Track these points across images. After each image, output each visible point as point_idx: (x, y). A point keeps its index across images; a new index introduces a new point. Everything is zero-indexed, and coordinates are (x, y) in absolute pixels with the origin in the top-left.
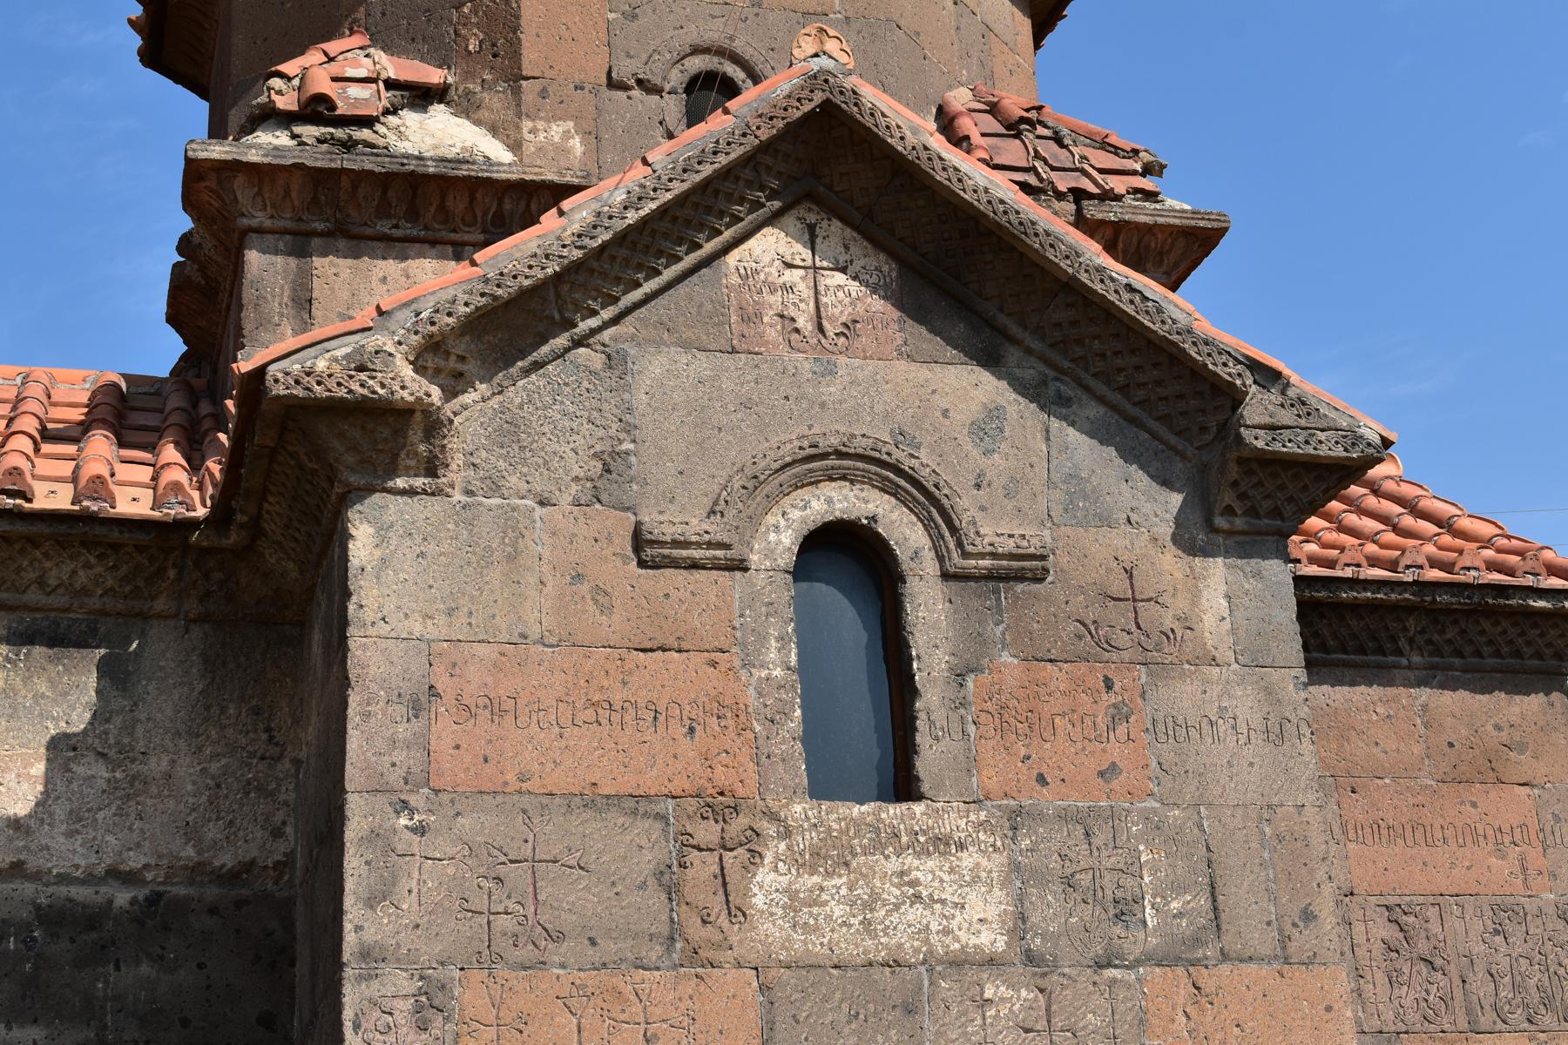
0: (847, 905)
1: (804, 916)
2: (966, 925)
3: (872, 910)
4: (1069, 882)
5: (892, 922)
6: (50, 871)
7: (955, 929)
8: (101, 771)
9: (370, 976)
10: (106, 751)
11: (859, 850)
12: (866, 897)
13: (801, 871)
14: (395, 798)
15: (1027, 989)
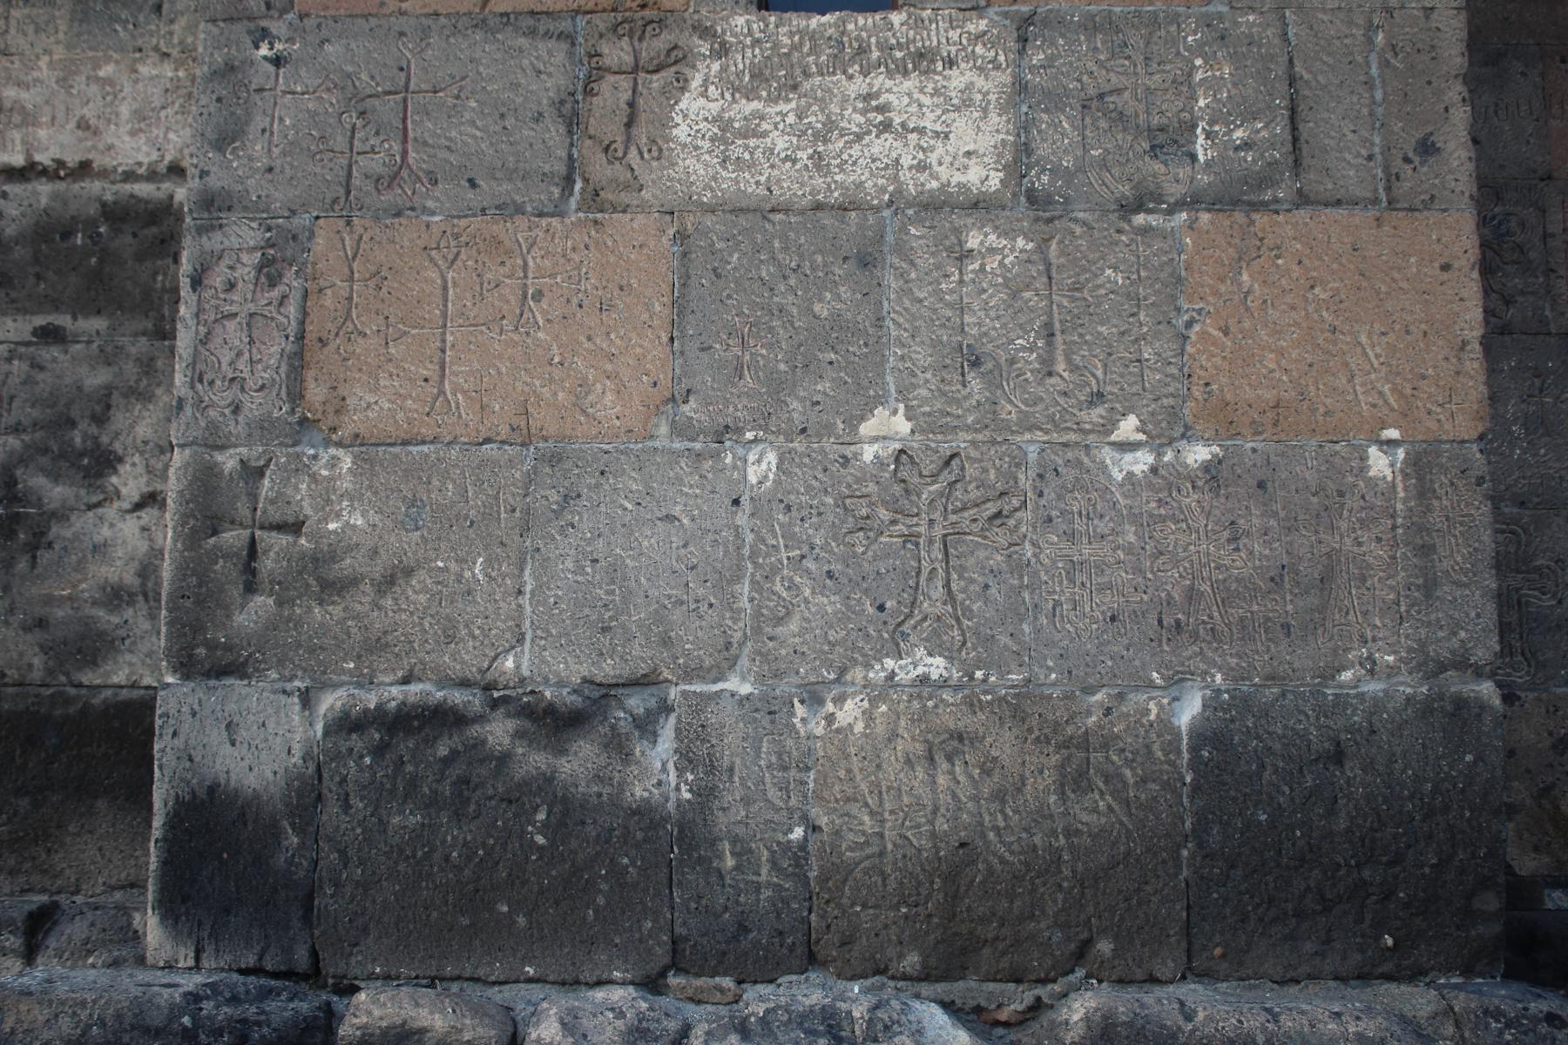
0: (794, 135)
1: (736, 150)
2: (948, 159)
3: (825, 142)
4: (1093, 103)
5: (851, 156)
6: (115, 168)
7: (935, 163)
8: (168, 71)
9: (213, 228)
10: (169, 51)
11: (814, 69)
12: (820, 126)
13: (737, 95)
14: (252, 26)
15: (1026, 237)
